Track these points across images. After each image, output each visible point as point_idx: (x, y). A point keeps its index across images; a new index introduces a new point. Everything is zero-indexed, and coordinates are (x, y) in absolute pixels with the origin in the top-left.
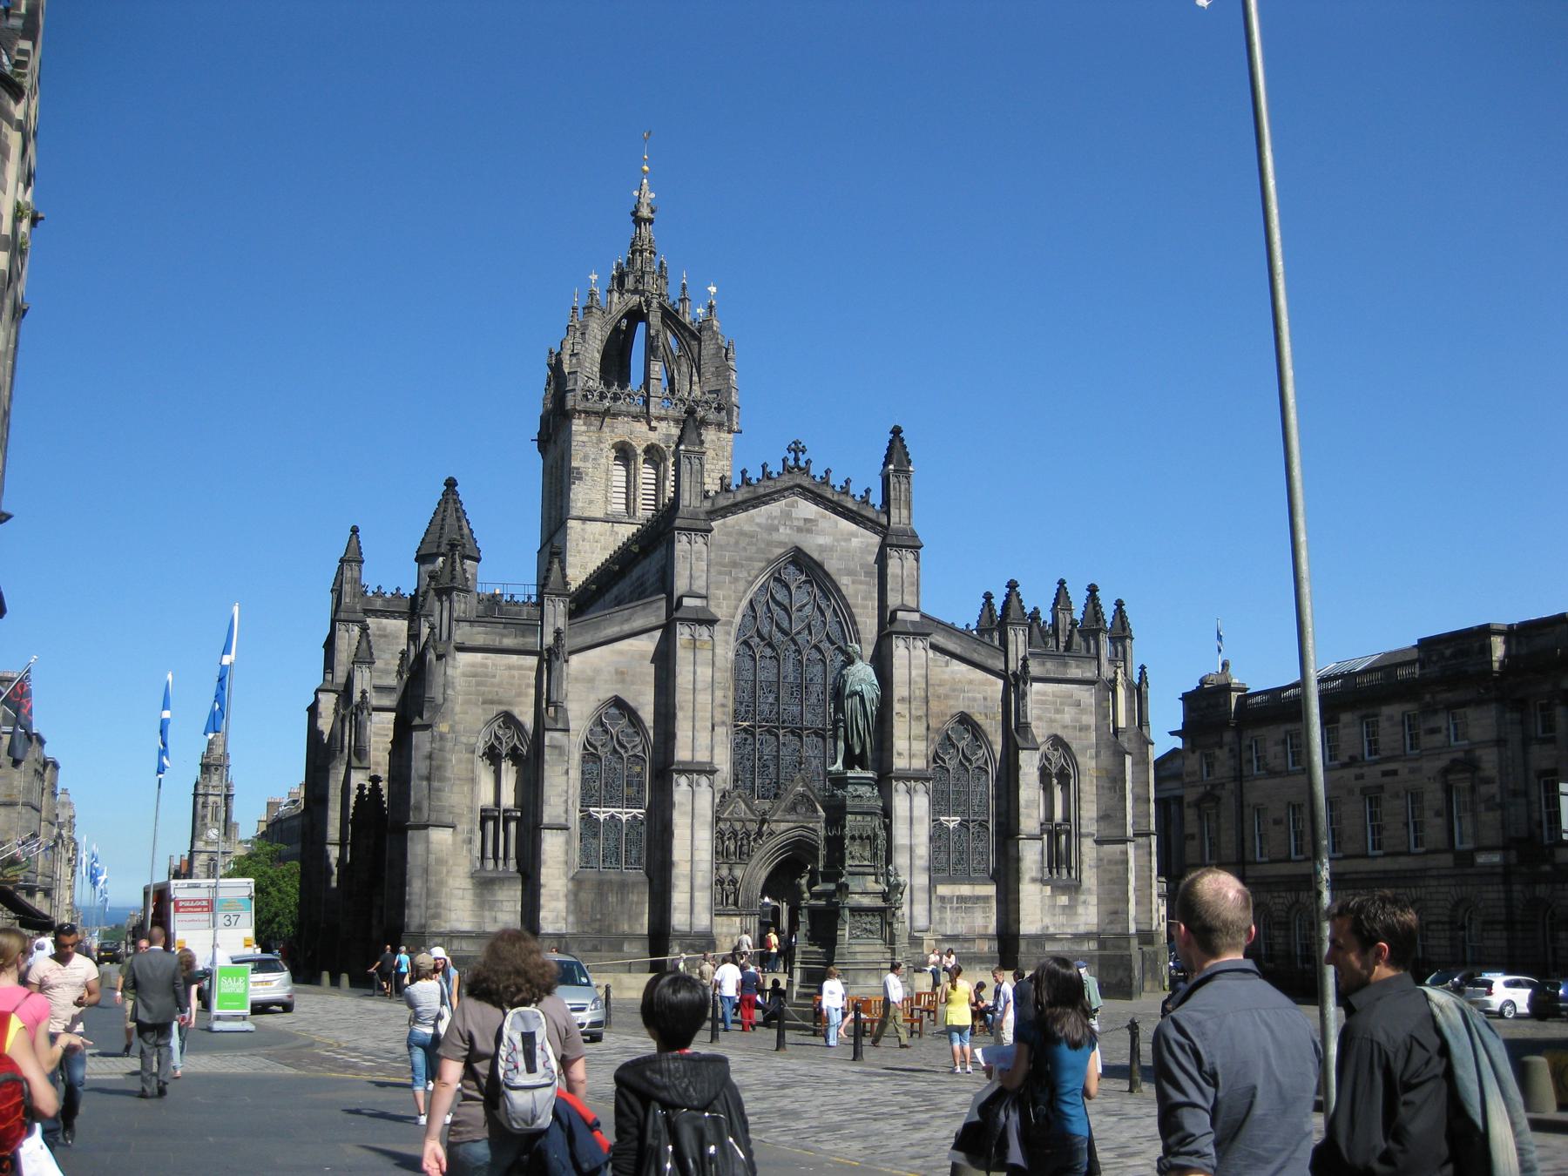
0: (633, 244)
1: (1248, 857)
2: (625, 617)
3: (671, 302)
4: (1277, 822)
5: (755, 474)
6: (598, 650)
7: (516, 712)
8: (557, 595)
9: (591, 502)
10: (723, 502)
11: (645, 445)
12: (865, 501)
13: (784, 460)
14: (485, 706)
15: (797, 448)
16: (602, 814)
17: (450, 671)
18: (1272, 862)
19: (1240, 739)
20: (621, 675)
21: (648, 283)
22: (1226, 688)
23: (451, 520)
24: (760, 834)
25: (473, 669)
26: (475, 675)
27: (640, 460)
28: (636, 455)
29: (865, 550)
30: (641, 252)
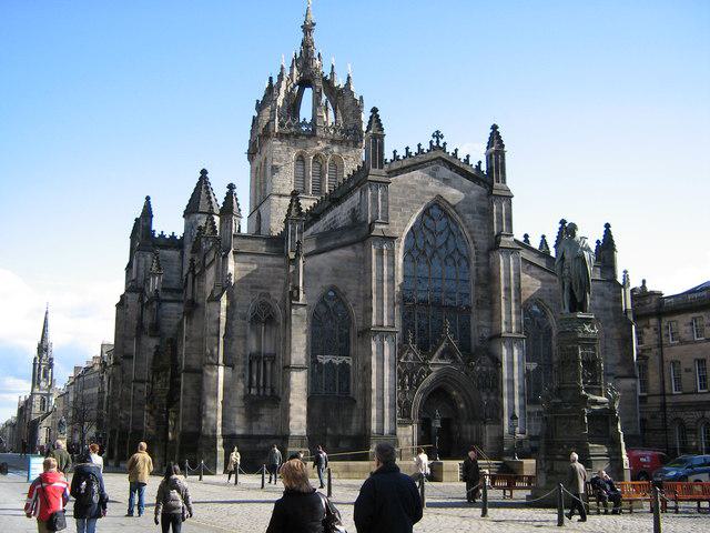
1: (667, 390)
4: (687, 370)
5: (414, 150)
7: (272, 293)
9: (284, 185)
10: (395, 166)
12: (478, 167)
13: (431, 142)
15: (438, 135)
16: (324, 360)
18: (684, 394)
19: (660, 320)
20: (336, 272)
22: (652, 293)
24: (422, 373)
29: (480, 198)
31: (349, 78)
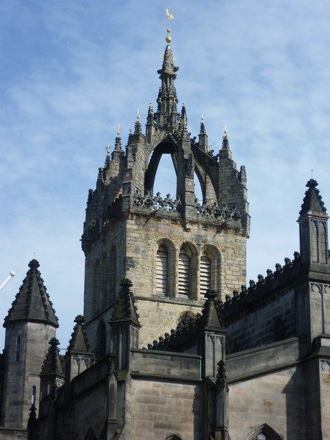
0: (160, 95)
2: (271, 354)
3: (192, 137)
6: (249, 382)
8: (216, 332)
9: (141, 285)
11: (181, 244)
14: (156, 430)
17: (128, 397)
21: (175, 122)
23: (35, 294)
25: (146, 395)
26: (148, 401)
27: (178, 253)
28: (175, 250)
30: (168, 99)
31: (225, 142)
